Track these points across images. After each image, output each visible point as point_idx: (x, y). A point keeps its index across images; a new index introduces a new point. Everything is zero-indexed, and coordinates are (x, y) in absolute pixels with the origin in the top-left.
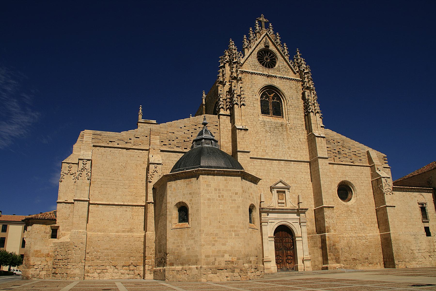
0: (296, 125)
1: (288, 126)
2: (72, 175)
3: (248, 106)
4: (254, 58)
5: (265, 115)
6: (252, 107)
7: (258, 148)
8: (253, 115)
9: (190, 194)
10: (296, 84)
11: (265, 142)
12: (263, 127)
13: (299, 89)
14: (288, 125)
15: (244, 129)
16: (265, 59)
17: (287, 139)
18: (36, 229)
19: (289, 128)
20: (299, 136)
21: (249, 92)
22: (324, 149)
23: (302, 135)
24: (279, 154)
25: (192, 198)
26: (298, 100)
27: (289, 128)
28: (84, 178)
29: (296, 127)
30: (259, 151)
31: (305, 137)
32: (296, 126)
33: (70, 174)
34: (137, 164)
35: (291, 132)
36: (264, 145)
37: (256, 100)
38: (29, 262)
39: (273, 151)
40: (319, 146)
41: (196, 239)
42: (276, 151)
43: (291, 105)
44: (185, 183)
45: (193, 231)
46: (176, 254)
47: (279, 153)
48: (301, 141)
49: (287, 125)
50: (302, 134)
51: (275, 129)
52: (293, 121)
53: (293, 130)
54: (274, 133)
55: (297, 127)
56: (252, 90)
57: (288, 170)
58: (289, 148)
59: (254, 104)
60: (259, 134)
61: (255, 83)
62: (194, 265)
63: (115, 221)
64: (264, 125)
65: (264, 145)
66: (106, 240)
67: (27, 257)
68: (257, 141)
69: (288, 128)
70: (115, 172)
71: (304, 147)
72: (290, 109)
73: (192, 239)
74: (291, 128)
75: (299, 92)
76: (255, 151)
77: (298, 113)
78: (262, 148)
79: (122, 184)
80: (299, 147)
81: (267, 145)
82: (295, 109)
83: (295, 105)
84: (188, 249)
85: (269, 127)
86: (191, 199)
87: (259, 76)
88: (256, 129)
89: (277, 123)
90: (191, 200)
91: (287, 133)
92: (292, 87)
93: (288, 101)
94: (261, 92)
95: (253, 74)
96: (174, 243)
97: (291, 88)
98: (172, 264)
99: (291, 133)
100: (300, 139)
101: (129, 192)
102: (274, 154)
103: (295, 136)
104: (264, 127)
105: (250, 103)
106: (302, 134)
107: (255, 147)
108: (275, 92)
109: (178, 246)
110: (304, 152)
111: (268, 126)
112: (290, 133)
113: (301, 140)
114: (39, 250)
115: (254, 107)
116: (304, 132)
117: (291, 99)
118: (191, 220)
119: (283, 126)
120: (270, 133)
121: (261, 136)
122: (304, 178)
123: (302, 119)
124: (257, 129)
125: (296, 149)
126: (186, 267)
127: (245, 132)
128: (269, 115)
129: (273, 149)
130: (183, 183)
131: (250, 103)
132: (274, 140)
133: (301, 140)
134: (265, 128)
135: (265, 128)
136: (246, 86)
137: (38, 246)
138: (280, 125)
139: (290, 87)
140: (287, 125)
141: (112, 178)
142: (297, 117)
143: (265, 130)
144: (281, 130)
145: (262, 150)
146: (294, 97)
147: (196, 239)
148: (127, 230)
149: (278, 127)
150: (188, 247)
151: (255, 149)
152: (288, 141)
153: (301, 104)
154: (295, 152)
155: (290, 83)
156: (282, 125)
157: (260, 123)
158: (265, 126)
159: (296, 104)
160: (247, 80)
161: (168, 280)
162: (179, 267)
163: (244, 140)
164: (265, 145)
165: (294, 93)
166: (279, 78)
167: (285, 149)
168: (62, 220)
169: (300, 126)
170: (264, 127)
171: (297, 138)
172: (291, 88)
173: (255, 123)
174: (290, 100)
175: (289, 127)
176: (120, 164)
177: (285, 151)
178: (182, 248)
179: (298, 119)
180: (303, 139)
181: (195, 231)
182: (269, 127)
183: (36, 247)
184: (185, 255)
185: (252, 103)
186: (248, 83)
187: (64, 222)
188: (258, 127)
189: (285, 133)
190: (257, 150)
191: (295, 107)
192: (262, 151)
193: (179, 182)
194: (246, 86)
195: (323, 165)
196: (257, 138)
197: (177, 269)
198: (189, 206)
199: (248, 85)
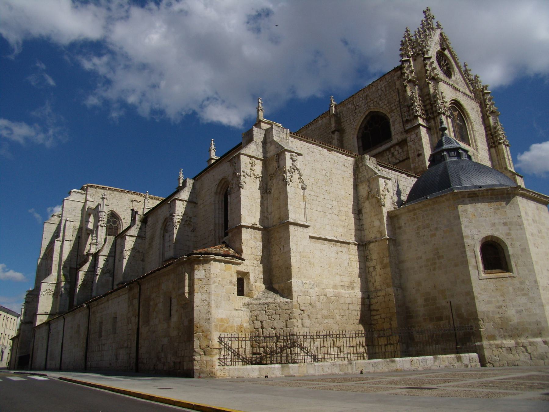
2: (256, 178)
9: (505, 224)
16: (442, 64)
18: (216, 276)
25: (510, 229)
28: (296, 186)
33: (255, 178)
34: (344, 177)
38: (210, 341)
41: (531, 295)
44: (491, 207)
45: (522, 283)
46: (498, 319)
62: (537, 337)
63: (330, 269)
66: (323, 301)
67: (203, 331)
70: (319, 185)
73: (525, 295)
79: (330, 206)
84: (519, 312)
86: (508, 231)
90: (508, 234)
96: (489, 302)
98: (492, 337)
101: (340, 220)
108: (458, 110)
109: (500, 307)
114: (225, 319)
118: (516, 265)
126: (522, 340)
130: (487, 207)
137: (223, 311)
141: (316, 194)
146: (477, 121)
147: (531, 295)
148: (347, 284)
150: (519, 309)
161: (491, 366)
162: (510, 342)
168: (253, 261)
176: (324, 172)
178: (507, 309)
181: (527, 282)
183: (220, 311)
184: (516, 321)
187: (256, 266)
193: (479, 205)
197: (506, 346)
198: (508, 243)
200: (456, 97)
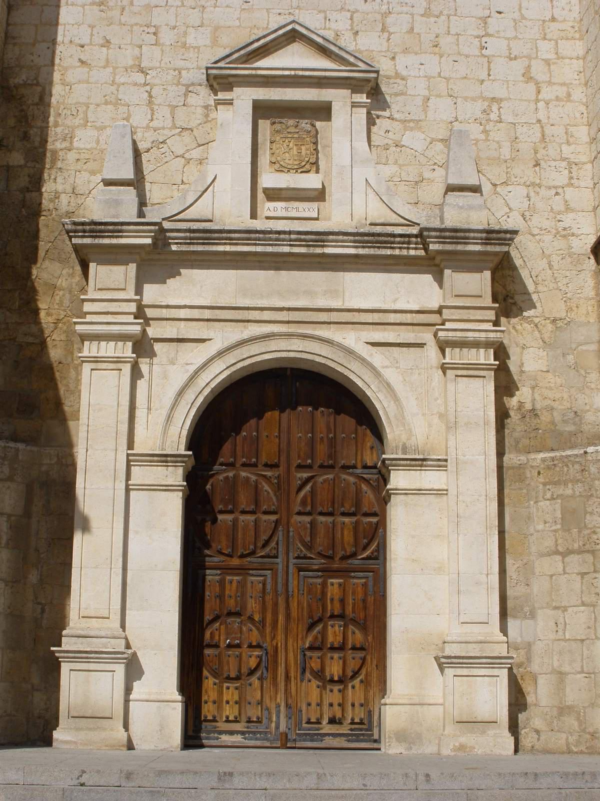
122: (516, 15)
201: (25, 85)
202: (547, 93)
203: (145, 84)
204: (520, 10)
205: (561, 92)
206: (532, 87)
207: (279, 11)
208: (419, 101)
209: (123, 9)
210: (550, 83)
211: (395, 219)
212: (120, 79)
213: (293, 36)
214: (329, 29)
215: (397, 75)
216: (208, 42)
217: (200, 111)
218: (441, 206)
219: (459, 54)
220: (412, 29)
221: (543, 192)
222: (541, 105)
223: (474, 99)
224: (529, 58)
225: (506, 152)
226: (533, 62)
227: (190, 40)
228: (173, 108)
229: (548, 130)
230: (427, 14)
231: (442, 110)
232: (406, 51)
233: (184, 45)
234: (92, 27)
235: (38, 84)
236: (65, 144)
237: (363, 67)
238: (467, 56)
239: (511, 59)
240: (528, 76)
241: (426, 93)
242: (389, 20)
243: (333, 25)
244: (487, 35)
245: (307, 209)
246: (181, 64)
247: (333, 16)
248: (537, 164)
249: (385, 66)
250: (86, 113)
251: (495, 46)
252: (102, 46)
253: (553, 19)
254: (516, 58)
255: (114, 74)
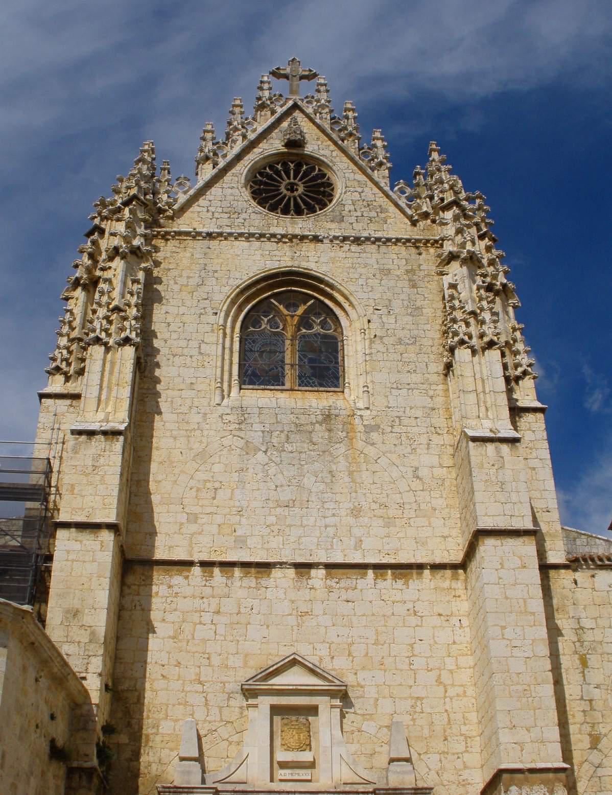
0: (401, 414)
1: (357, 421)
3: (174, 356)
4: (233, 188)
5: (262, 387)
6: (191, 357)
7: (199, 521)
8: (195, 387)
10: (408, 256)
11: (237, 492)
12: (234, 432)
13: (422, 274)
14: (361, 416)
15: (105, 433)
17: (351, 473)
19: (365, 426)
20: (412, 457)
21: (188, 303)
22: (514, 495)
23: (431, 451)
24: (303, 540)
26: (413, 316)
27: (365, 426)
29: (397, 420)
30: (200, 533)
31: (445, 457)
32: (399, 417)
35: (373, 444)
36: (232, 503)
37: (213, 331)
39: (275, 528)
40: (486, 481)
42: (290, 526)
43: (381, 338)
47: (300, 537)
48: (421, 479)
49: (354, 415)
50: (428, 449)
51: (292, 436)
52: (387, 396)
53: (383, 433)
54: (283, 454)
55: (405, 421)
56: (201, 293)
57: (346, 608)
58: (356, 512)
59: (203, 346)
60: (211, 460)
61: (219, 268)
64: (239, 424)
65: (232, 503)
68: (197, 491)
69: (361, 428)
71: (439, 503)
72: (374, 351)
74: (376, 428)
75: (420, 284)
76: (184, 530)
77: (412, 366)
78: (218, 519)
80: (410, 503)
81: (244, 504)
82: (401, 348)
83: (401, 334)
85: (263, 432)
87: (242, 244)
88: (201, 442)
89: (305, 412)
91: (351, 447)
92: (389, 270)
93: (369, 321)
94: (248, 300)
95: (215, 238)
97: (385, 272)
99: (371, 447)
100: (417, 469)
102: (275, 542)
103: (394, 457)
104: (237, 433)
105: (183, 343)
106: (428, 449)
107: (183, 518)
110: (437, 522)
111: (257, 427)
112: (370, 450)
113: (424, 472)
115: (200, 357)
116: (436, 439)
117: (384, 311)
119: (333, 422)
120: (265, 452)
121: (217, 468)
122: (432, 642)
123: (434, 387)
124: (204, 440)
125: (391, 513)
127: (108, 443)
128: (283, 384)
129: (272, 519)
131: (183, 343)
132: (280, 479)
133: (420, 474)
134: (242, 434)
135: (242, 434)
136: (176, 283)
138: (320, 418)
139: (381, 271)
140: (354, 415)
142: (406, 378)
143: (241, 443)
144: (322, 438)
145: (219, 525)
146: (396, 304)
149: (309, 428)
151: (181, 524)
152: (352, 482)
153: (428, 327)
154: (387, 525)
155: (379, 256)
156: (329, 416)
157: (221, 416)
158: (243, 426)
159: (403, 329)
160: (186, 262)
163: (98, 478)
164: (237, 504)
165: (397, 290)
166: (331, 241)
167: (334, 515)
169: (419, 413)
170: (240, 429)
171: (401, 468)
172: (385, 272)
173: (197, 418)
174: (374, 318)
175: (366, 423)
177: (335, 526)
179: (412, 386)
180: (432, 467)
182: (263, 432)
185: (194, 344)
186: (185, 274)
188: (212, 433)
189: (342, 449)
190: (193, 528)
191: (400, 341)
192: (214, 529)
194: (176, 283)
195: (506, 566)
196: (201, 476)
199: (188, 277)
200: (290, 264)
201: (128, 690)
202: (451, 692)
203: (203, 692)
204: (434, 638)
205: (460, 690)
206: (441, 688)
207: (285, 644)
208: (372, 701)
209: (188, 642)
210: (453, 685)
211: (358, 780)
212: (187, 688)
213: (294, 663)
214: (316, 655)
215: (359, 685)
216: (241, 665)
217: (237, 710)
218: (387, 770)
219: (396, 669)
220: (367, 653)
221: (450, 757)
222: (448, 700)
223: (406, 699)
224: (440, 669)
225: (426, 732)
226: (442, 672)
227: (230, 663)
228: (221, 708)
229: (452, 716)
230: (376, 643)
231: (386, 706)
232: (363, 668)
233: (226, 666)
234: (169, 653)
235: (136, 690)
236: (154, 731)
237: (338, 683)
238: (401, 670)
239: (428, 671)
240: (439, 682)
241: (377, 696)
242: (353, 648)
243: (318, 653)
244: (414, 655)
245: (304, 774)
246: (225, 679)
247: (318, 646)
248: (446, 739)
249: (350, 679)
250: (166, 710)
251: (419, 662)
252: (176, 666)
253: (454, 643)
254: (431, 670)
255: (183, 684)
